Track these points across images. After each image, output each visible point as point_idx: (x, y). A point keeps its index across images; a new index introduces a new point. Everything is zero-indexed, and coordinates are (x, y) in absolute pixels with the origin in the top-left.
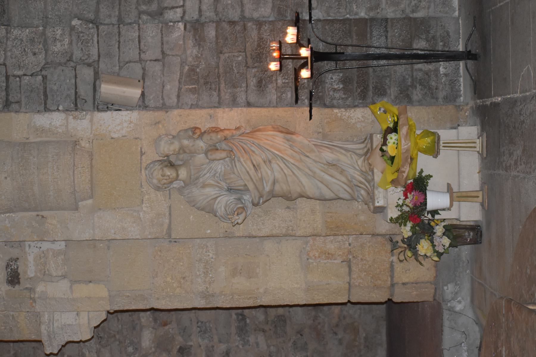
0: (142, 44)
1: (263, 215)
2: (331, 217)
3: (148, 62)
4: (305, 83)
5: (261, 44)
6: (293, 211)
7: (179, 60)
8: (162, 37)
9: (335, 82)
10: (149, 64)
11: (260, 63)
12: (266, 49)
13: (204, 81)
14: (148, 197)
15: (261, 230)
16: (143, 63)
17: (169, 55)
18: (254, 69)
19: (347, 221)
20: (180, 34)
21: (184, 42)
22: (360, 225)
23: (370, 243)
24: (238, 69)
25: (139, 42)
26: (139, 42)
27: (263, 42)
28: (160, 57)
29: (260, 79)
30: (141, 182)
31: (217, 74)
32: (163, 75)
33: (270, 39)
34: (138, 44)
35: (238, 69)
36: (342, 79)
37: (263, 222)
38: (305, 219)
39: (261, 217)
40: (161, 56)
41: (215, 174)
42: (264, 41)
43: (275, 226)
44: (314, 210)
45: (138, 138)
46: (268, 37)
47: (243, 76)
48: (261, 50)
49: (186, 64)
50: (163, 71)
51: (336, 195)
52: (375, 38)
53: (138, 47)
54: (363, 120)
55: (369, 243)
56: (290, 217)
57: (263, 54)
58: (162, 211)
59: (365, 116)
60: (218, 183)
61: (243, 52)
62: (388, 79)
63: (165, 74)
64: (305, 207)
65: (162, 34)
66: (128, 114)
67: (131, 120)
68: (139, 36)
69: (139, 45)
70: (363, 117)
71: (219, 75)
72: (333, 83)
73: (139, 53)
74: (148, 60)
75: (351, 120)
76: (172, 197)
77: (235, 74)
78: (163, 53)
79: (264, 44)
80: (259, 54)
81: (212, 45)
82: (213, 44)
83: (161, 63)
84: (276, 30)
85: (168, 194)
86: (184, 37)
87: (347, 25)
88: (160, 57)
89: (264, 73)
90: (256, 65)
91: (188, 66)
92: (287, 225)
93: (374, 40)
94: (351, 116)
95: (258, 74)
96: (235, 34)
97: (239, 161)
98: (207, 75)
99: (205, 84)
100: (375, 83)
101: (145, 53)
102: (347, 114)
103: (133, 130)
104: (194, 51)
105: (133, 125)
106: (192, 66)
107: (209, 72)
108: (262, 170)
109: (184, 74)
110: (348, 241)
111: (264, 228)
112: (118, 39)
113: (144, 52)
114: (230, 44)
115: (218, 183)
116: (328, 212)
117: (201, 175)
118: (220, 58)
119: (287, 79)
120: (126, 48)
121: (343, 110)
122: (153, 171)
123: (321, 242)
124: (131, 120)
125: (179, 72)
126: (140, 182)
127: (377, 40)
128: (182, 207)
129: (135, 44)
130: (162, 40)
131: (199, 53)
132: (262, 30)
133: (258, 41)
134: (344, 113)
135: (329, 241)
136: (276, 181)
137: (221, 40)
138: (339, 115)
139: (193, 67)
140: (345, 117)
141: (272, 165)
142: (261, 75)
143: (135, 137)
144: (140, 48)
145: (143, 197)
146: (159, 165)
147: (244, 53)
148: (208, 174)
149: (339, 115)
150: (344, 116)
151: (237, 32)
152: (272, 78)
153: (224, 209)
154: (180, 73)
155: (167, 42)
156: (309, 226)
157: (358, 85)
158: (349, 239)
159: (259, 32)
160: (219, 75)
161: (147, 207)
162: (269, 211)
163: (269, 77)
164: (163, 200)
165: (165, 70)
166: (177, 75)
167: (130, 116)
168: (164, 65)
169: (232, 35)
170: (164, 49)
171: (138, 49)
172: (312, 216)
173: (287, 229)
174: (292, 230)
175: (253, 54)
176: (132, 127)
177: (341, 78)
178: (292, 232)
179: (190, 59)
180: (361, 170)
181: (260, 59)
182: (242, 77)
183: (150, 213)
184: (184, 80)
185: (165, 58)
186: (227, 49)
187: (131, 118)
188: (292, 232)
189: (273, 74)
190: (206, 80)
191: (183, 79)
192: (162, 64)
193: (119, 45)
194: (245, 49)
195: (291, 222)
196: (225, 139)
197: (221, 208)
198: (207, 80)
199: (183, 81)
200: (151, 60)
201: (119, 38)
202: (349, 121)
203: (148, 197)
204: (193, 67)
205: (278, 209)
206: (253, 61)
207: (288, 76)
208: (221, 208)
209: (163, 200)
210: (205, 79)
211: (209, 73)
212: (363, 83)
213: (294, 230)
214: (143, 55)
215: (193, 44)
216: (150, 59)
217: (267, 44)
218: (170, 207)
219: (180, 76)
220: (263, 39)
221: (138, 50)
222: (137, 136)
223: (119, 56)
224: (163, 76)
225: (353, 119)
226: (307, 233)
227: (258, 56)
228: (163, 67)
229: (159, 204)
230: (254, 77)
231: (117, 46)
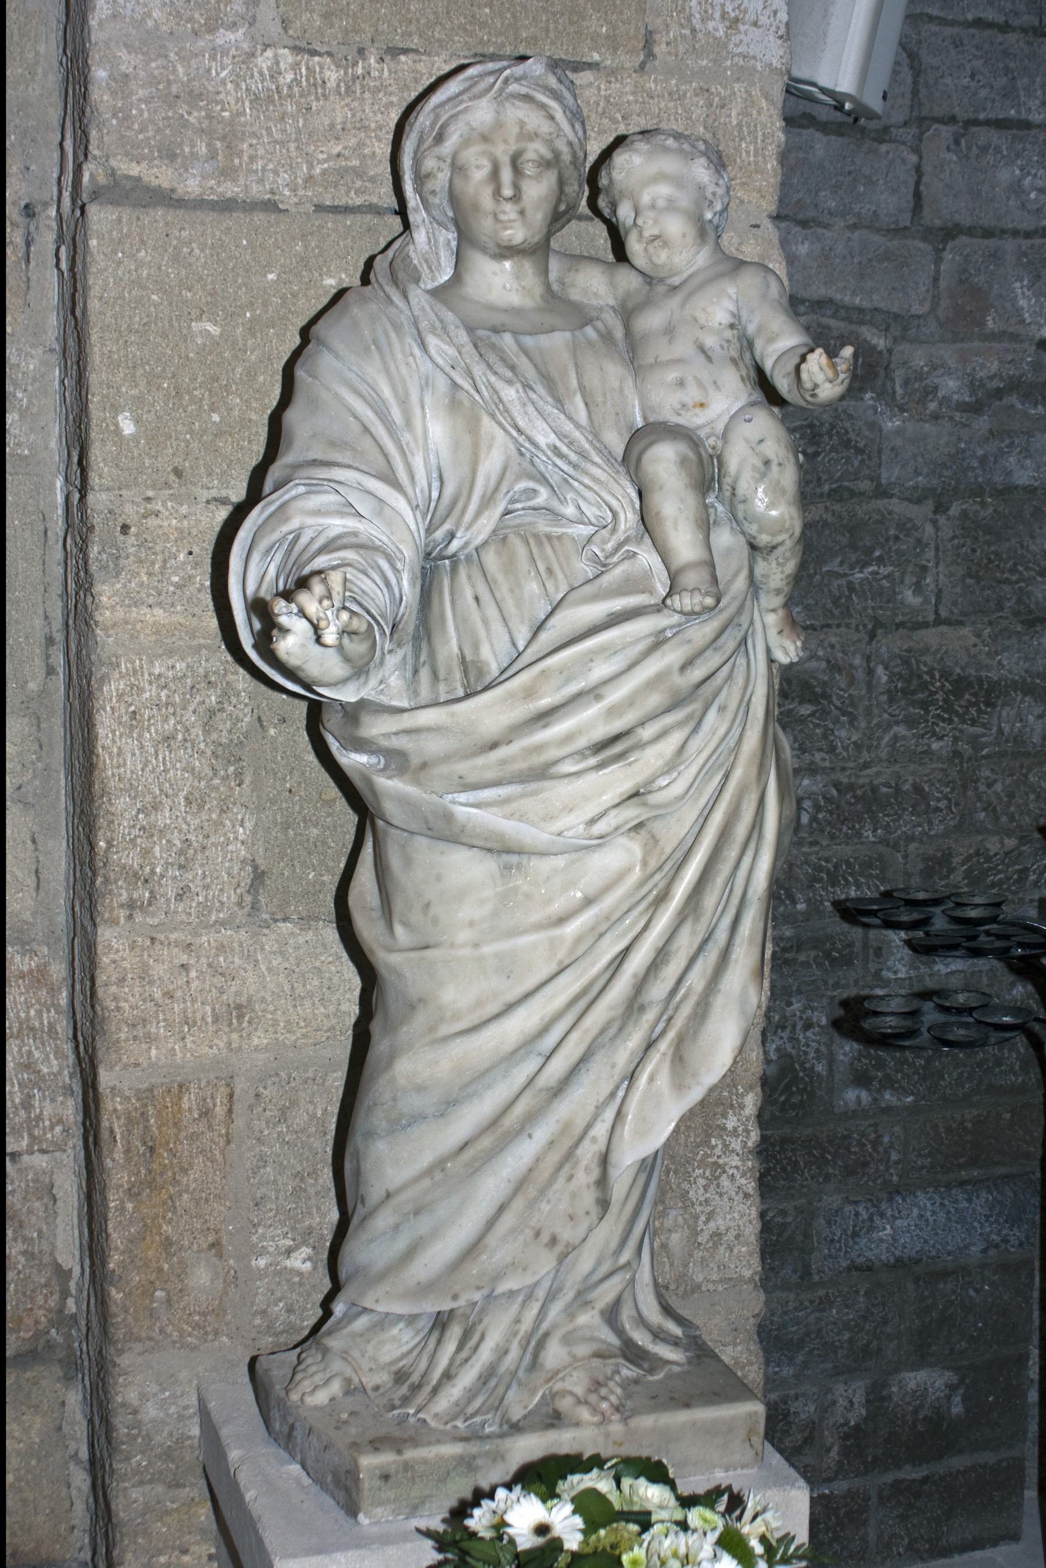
0: (993, 136)
1: (214, 736)
2: (206, 1113)
3: (913, 158)
4: (794, 902)
5: (967, 697)
6: (240, 904)
7: (917, 309)
8: (1015, 233)
9: (791, 1039)
10: (904, 161)
11: (889, 691)
12: (944, 720)
13: (822, 425)
14: (331, 84)
15: (132, 728)
16: (908, 134)
17: (938, 260)
18: (865, 664)
19: (185, 1196)
20: (1028, 320)
21: (993, 337)
22: (160, 1270)
23: (22, 1259)
24: (866, 588)
25: (1000, 124)
26: (1000, 124)
27: (976, 704)
28: (930, 218)
29: (818, 690)
30: (416, 51)
31: (848, 489)
32: (855, 227)
33: (984, 735)
34: (992, 116)
35: (866, 588)
36: (804, 1069)
37: (180, 737)
38: (193, 974)
39: (208, 727)
40: (938, 223)
41: (544, 480)
42: (980, 711)
43: (156, 807)
44: (240, 1017)
45: (650, 55)
46: (995, 729)
47: (836, 612)
48: (940, 696)
49: (895, 340)
50: (871, 225)
51: (388, 1196)
52: (965, 1204)
53: (982, 116)
54: (703, 1238)
55: (24, 1253)
56: (207, 887)
57: (924, 705)
58: (252, 159)
59: (722, 1249)
60: (487, 501)
61: (936, 612)
62: (795, 1278)
63: (857, 235)
64: (263, 968)
65: (1028, 235)
66: (775, 13)
67: (742, 28)
68: (1027, 125)
69: (987, 123)
70: (717, 1236)
71: (846, 495)
72: (786, 1034)
73: (952, 120)
74: (921, 158)
75: (701, 1182)
76: (330, 221)
77: (845, 575)
78: (949, 233)
79: (966, 713)
80: (924, 686)
81: (974, 469)
82: (979, 472)
83: (905, 220)
84: (1021, 767)
85: (342, 202)
86: (1015, 337)
87: (1020, 1079)
88: (930, 218)
89: (844, 713)
90: (880, 670)
91: (890, 351)
92: (162, 876)
93: (956, 1201)
94: (725, 1182)
95: (843, 686)
96: (1014, 578)
97: (658, 642)
98: (849, 441)
99: (811, 426)
100: (779, 1219)
101: (953, 147)
102: (735, 1161)
103: (694, 31)
104: (952, 384)
105: (721, 33)
106: (886, 368)
107: (859, 451)
108: (592, 777)
109: (853, 327)
110: (30, 1145)
111: (142, 747)
112: (1016, 23)
113: (957, 142)
114: (974, 550)
115: (487, 501)
116: (231, 1096)
117: (534, 396)
118: (919, 501)
119: (814, 819)
120: (975, 57)
121: (755, 1136)
122: (543, 106)
123: (23, 1015)
124: (742, 28)
125: (866, 304)
126: (415, 42)
127: (956, 1210)
128: (271, 277)
129: (993, 101)
130: (1003, 232)
131: (941, 404)
132: (1022, 701)
133: (980, 681)
134: (736, 1145)
135: (30, 1053)
136: (514, 859)
137: (990, 510)
138: (731, 1123)
139: (882, 373)
140: (718, 1151)
141: (623, 840)
142: (834, 699)
143: (657, 37)
144: (977, 123)
145: (329, 54)
146: (570, 144)
147: (931, 617)
148: (553, 438)
149: (731, 1123)
150: (726, 1146)
151: (1023, 585)
152: (821, 750)
153: (332, 533)
154: (861, 310)
155: (995, 256)
156: (158, 994)
157: (773, 1145)
158: (43, 1151)
159: (1015, 686)
160: (846, 495)
161: (275, 73)
162: (239, 774)
163: (825, 736)
164: (311, 166)
165: (876, 238)
166: (854, 294)
167: (763, 20)
168: (898, 232)
169: (1010, 564)
170: (964, 239)
171: (972, 116)
172: (208, 1009)
173: (136, 875)
174: (131, 905)
175: (928, 659)
176: (711, 25)
177: (807, 1065)
178: (122, 906)
179: (919, 359)
180: (547, 1335)
181: (903, 690)
182: (829, 605)
183: (237, 85)
184: (828, 328)
185: (924, 239)
186: (954, 537)
187: (755, 24)
188: (122, 906)
189: (837, 755)
190: (829, 433)
191: (832, 323)
192: (902, 225)
193: (990, 25)
194: (948, 622)
195: (179, 897)
196: (753, 547)
197: (341, 514)
198: (826, 438)
199: (825, 321)
200: (918, 170)
201: (1024, 30)
202: (698, 1172)
203: (331, 84)
204: (882, 373)
205: (248, 825)
206: (900, 657)
207: (829, 823)
208: (348, 509)
209: (311, 166)
210: (833, 427)
211: (856, 448)
212: (783, 1169)
213: (130, 917)
214: (946, 132)
215: (981, 380)
216: (927, 169)
217: (964, 722)
218: (271, 206)
219: (847, 308)
220: (988, 704)
221: (965, 117)
222: (660, 49)
223: (943, 22)
224: (848, 227)
225: (706, 1188)
226: (113, 989)
227: (915, 682)
228: (888, 230)
229: (292, 146)
230: (828, 661)
231: (990, 15)
